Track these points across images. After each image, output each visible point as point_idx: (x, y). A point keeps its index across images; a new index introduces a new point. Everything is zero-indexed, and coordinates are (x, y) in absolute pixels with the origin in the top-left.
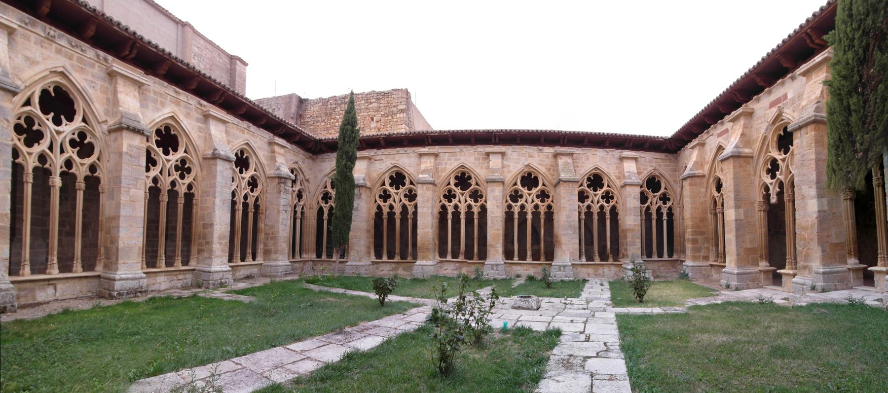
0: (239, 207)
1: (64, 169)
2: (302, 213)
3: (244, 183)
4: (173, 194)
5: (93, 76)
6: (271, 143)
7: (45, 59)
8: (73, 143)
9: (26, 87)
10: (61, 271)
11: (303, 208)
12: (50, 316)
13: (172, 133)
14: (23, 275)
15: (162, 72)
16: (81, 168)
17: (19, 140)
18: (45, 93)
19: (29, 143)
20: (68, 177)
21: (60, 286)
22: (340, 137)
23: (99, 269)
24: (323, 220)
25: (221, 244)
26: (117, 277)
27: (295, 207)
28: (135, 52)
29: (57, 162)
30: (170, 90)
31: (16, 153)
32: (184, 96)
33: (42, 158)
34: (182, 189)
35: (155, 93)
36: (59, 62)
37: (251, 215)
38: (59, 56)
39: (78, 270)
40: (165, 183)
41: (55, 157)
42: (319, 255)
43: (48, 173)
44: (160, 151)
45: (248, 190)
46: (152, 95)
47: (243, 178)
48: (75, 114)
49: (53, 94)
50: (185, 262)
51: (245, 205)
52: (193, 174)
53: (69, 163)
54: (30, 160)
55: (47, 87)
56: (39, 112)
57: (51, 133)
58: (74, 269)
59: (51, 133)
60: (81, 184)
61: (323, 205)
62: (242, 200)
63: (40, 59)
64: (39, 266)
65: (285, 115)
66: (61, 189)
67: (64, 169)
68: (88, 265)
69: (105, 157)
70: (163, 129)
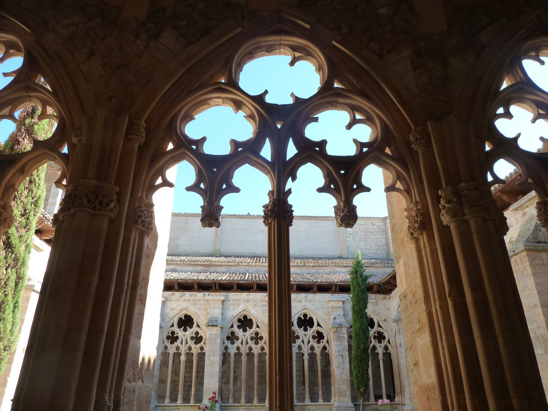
1: (188, 351)
5: (200, 305)
8: (192, 338)
18: (180, 319)
19: (172, 343)
20: (189, 355)
33: (178, 348)
35: (233, 300)
40: (244, 350)
46: (232, 302)
54: (172, 349)
63: (176, 307)
67: (188, 351)
70: (242, 318)
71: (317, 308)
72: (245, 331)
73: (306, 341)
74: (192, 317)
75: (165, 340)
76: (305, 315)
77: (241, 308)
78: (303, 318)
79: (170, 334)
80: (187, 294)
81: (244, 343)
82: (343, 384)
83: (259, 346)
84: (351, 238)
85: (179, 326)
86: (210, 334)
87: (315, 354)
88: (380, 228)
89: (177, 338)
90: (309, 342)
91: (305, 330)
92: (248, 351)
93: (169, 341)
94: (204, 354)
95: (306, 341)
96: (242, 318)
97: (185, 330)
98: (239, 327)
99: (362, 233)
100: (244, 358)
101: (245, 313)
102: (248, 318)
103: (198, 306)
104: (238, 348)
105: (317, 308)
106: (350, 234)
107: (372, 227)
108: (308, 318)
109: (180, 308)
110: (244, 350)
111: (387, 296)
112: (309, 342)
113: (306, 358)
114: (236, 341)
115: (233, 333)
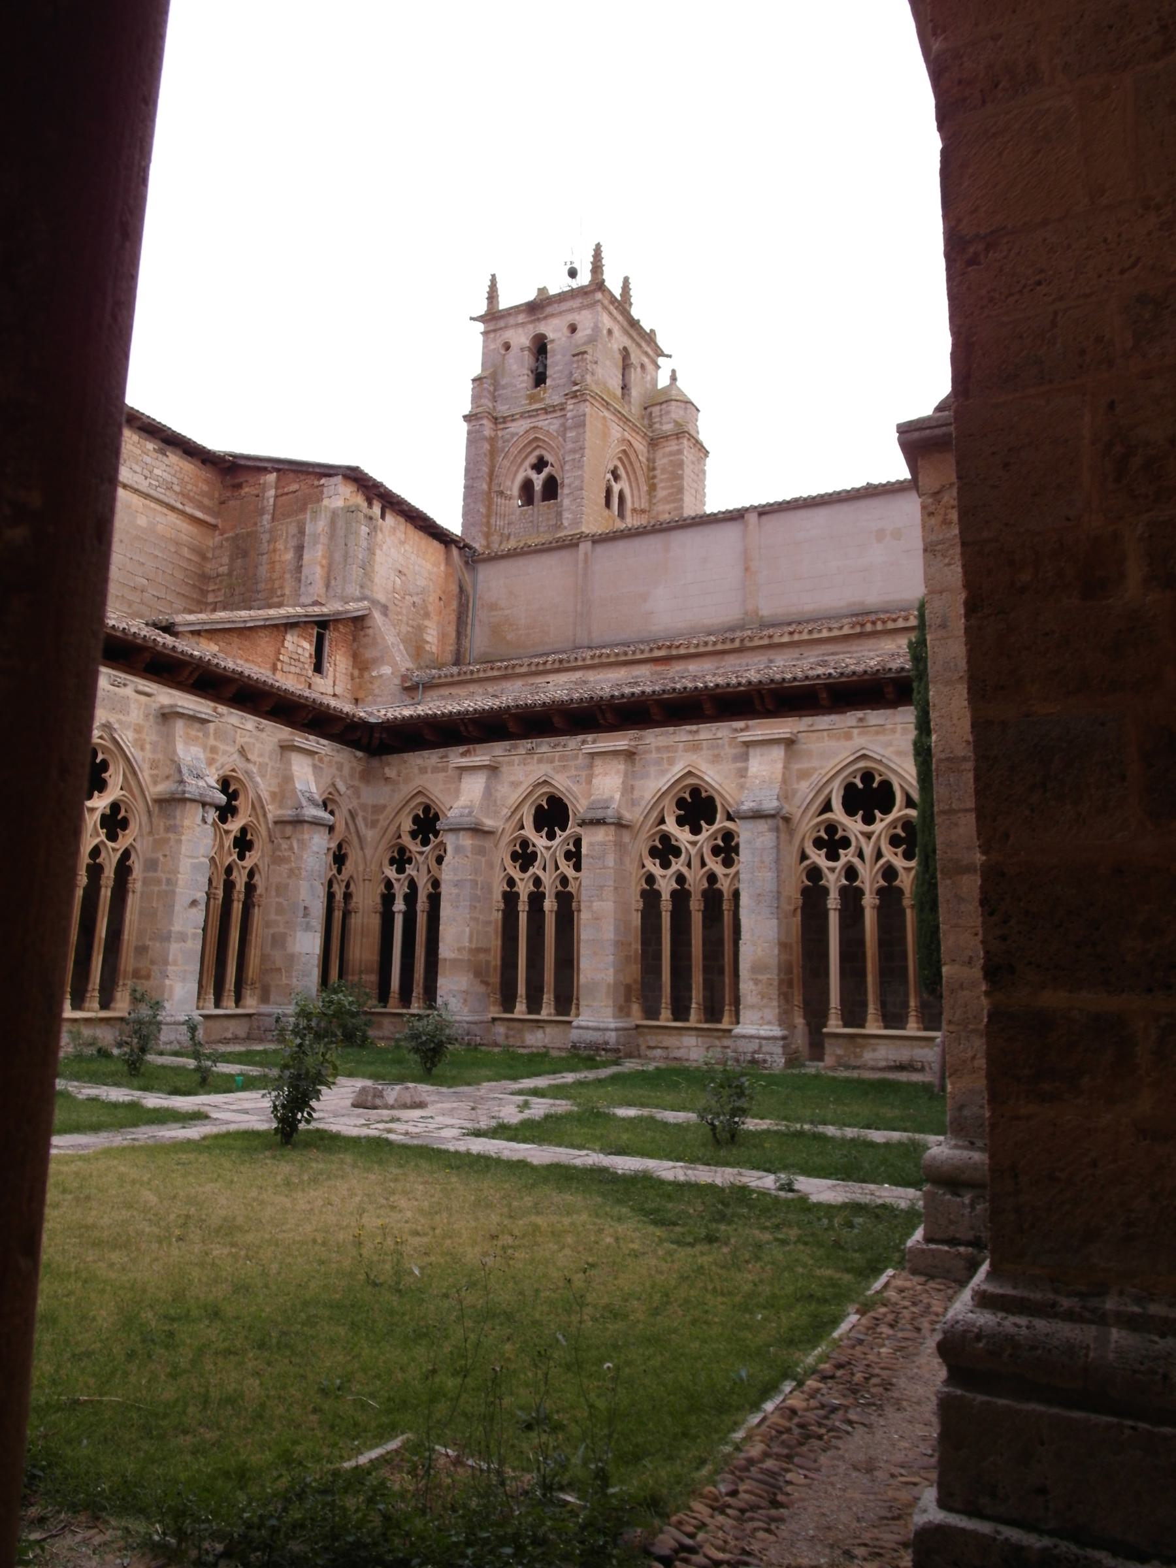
1: (560, 888)
13: (704, 795)
19: (524, 869)
25: (756, 982)
30: (681, 735)
31: (511, 882)
32: (707, 732)
35: (658, 749)
46: (654, 755)
67: (560, 888)
70: (687, 796)
72: (696, 831)
73: (868, 850)
74: (566, 801)
76: (867, 776)
77: (677, 770)
78: (860, 786)
80: (544, 746)
81: (696, 862)
87: (900, 891)
89: (533, 857)
90: (879, 855)
91: (869, 820)
92: (706, 885)
95: (868, 850)
96: (687, 796)
100: (696, 905)
101: (691, 781)
102: (704, 795)
103: (574, 773)
104: (681, 879)
108: (875, 785)
109: (532, 779)
110: (696, 881)
112: (879, 855)
113: (869, 901)
115: (665, 838)
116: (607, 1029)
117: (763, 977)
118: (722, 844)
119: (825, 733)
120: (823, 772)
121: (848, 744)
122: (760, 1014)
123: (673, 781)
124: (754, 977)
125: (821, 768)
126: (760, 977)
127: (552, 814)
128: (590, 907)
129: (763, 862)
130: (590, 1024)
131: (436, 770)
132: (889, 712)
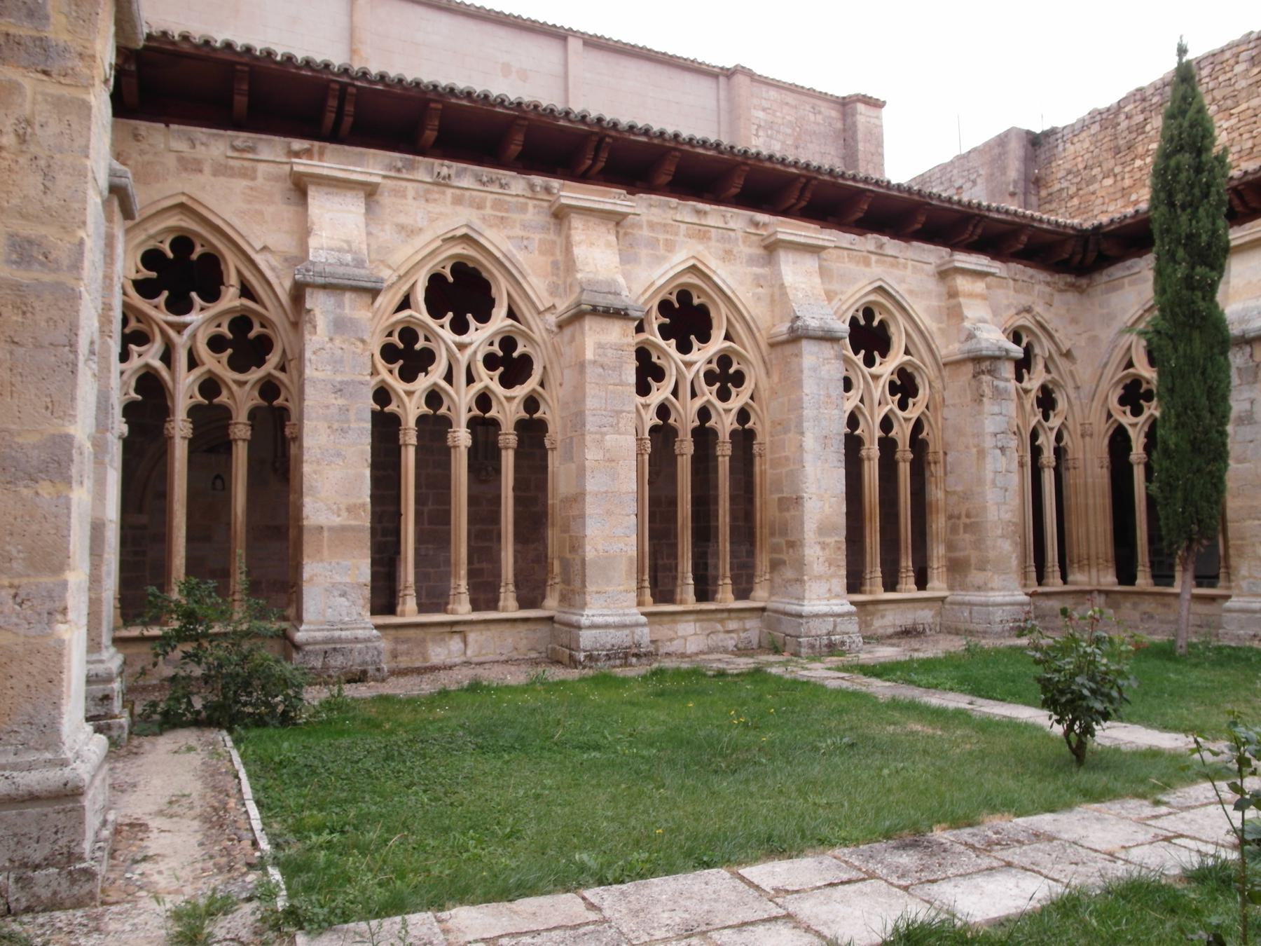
0: (872, 451)
1: (476, 412)
2: (1059, 452)
3: (879, 389)
4: (704, 436)
5: (524, 227)
6: (944, 274)
7: (432, 220)
8: (491, 362)
9: (400, 277)
10: (476, 607)
11: (1059, 438)
12: (444, 693)
14: (403, 615)
15: (664, 179)
16: (508, 407)
17: (391, 372)
18: (436, 280)
19: (408, 375)
20: (483, 427)
21: (472, 636)
22: (1155, 202)
23: (551, 605)
24: (1130, 467)
25: (824, 546)
26: (584, 621)
27: (1034, 435)
28: (604, 156)
29: (461, 400)
30: (683, 211)
31: (382, 395)
32: (719, 217)
33: (434, 398)
34: (724, 423)
35: (652, 226)
36: (457, 218)
37: (904, 470)
38: (459, 209)
39: (509, 607)
41: (457, 393)
42: (1126, 574)
43: (446, 423)
44: (670, 346)
45: (892, 404)
46: (646, 232)
47: (876, 378)
48: (493, 306)
49: (451, 279)
50: (743, 592)
51: (887, 446)
52: (748, 386)
53: (484, 400)
54: (410, 404)
55: (439, 269)
56: (425, 316)
57: (448, 349)
58: (501, 604)
59: (448, 349)
60: (508, 438)
61: (1126, 420)
62: (878, 433)
64: (433, 599)
65: (992, 194)
66: (470, 450)
67: (476, 412)
68: (530, 596)
69: (553, 380)
71: (911, 292)
75: (381, 364)
77: (678, 260)
79: (395, 339)
82: (1003, 536)
83: (735, 403)
84: (761, 140)
85: (436, 311)
86: (600, 346)
88: (830, 125)
89: (428, 357)
92: (697, 423)
93: (396, 368)
94: (541, 426)
96: (674, 298)
97: (460, 327)
98: (665, 332)
99: (789, 131)
103: (518, 232)
105: (911, 292)
106: (759, 126)
107: (812, 117)
111: (1083, 282)
114: (654, 385)
116: (637, 625)
117: (831, 540)
118: (718, 370)
119: (845, 253)
120: (844, 298)
121: (867, 270)
122: (827, 586)
123: (671, 274)
124: (822, 540)
125: (842, 293)
126: (828, 540)
127: (462, 290)
128: (600, 442)
129: (829, 396)
130: (611, 620)
131: (221, 170)
132: (903, 244)
